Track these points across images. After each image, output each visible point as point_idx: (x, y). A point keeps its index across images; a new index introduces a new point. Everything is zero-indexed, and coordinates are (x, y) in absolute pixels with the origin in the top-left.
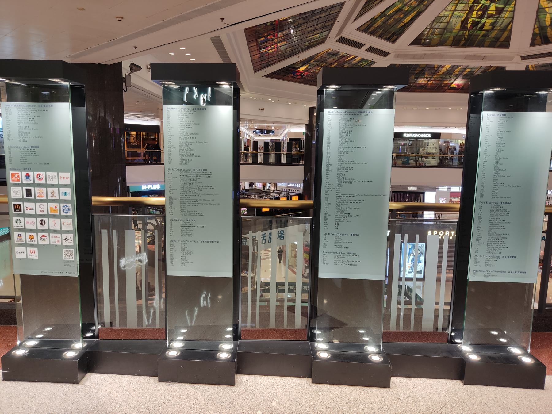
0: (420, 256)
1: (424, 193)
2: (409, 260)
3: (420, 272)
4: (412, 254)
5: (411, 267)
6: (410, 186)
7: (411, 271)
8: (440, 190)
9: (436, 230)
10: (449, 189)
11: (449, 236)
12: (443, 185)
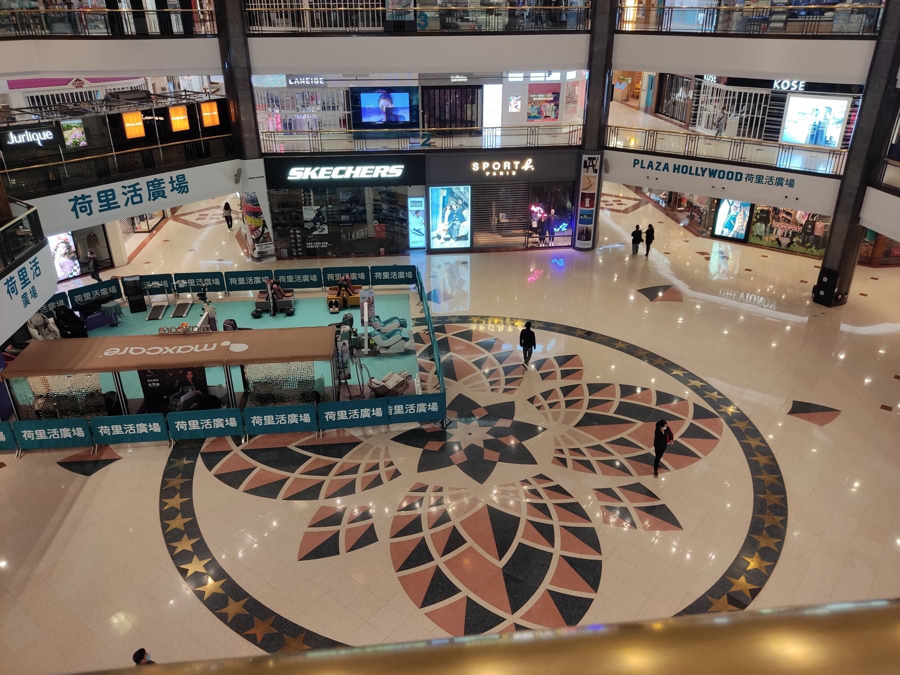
0: (464, 209)
1: (481, 87)
2: (443, 217)
3: (464, 238)
4: (448, 207)
5: (449, 230)
6: (455, 75)
7: (449, 236)
8: (510, 80)
9: (486, 161)
10: (527, 77)
11: (510, 171)
12: (516, 70)
